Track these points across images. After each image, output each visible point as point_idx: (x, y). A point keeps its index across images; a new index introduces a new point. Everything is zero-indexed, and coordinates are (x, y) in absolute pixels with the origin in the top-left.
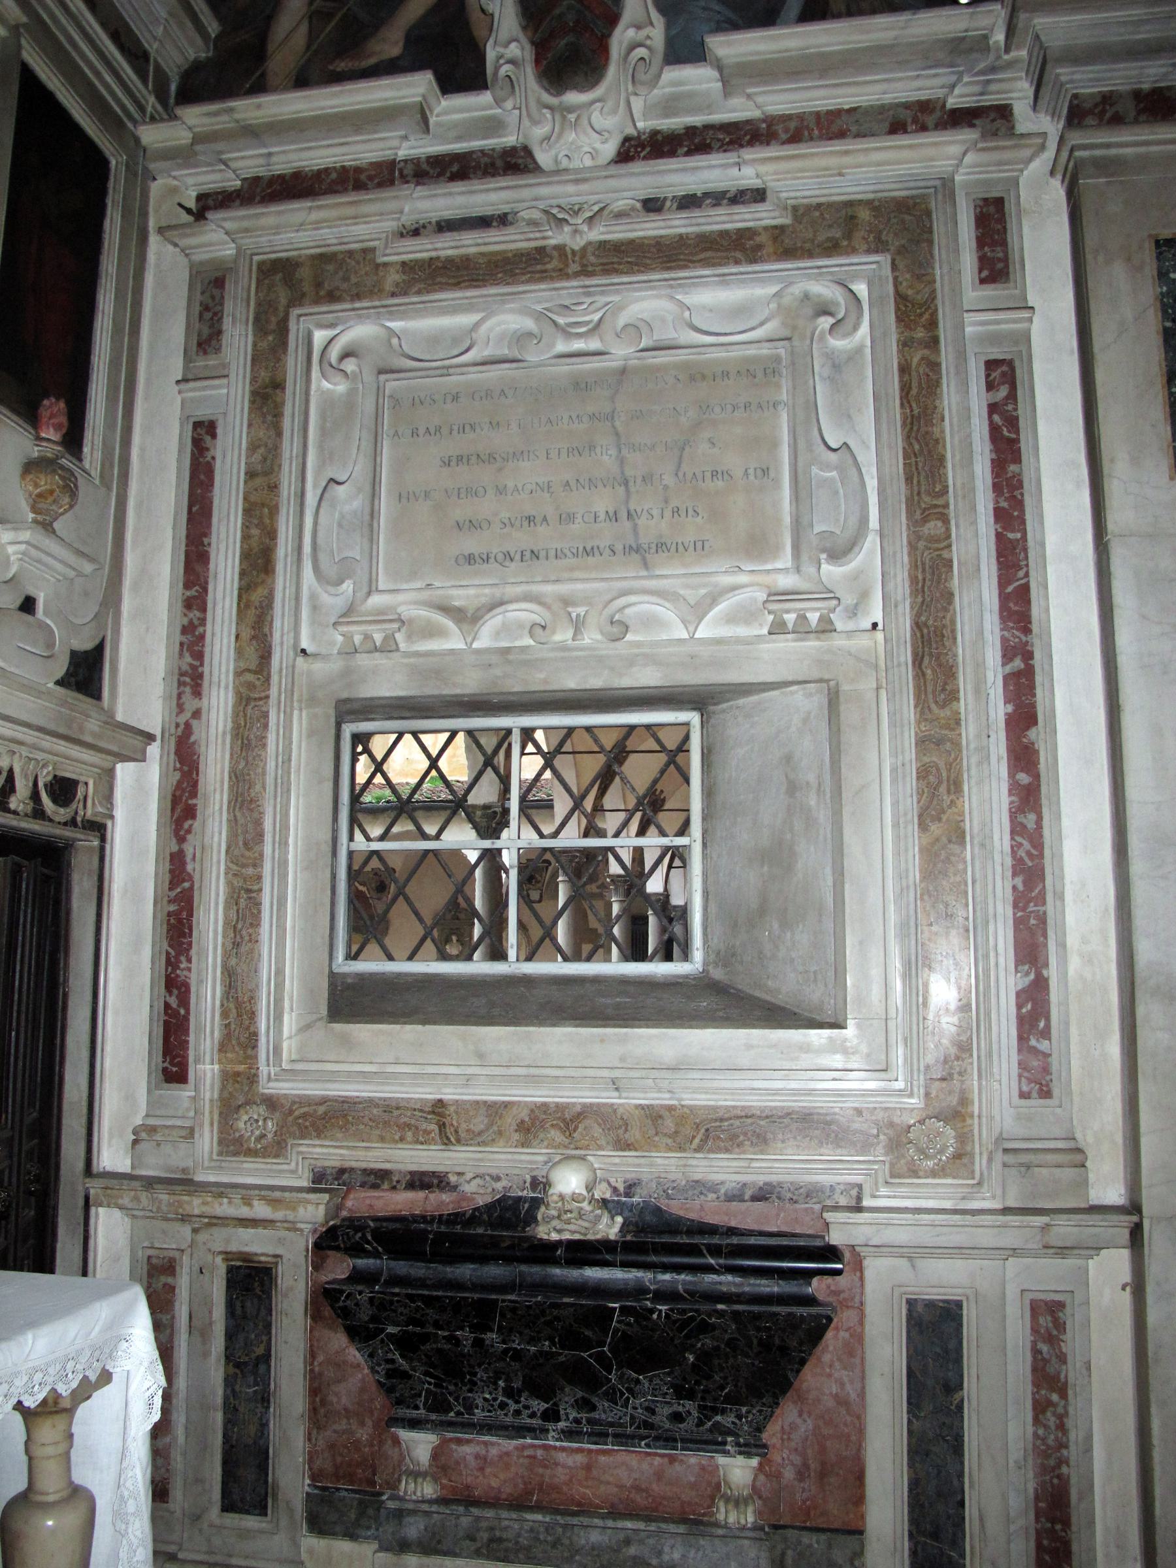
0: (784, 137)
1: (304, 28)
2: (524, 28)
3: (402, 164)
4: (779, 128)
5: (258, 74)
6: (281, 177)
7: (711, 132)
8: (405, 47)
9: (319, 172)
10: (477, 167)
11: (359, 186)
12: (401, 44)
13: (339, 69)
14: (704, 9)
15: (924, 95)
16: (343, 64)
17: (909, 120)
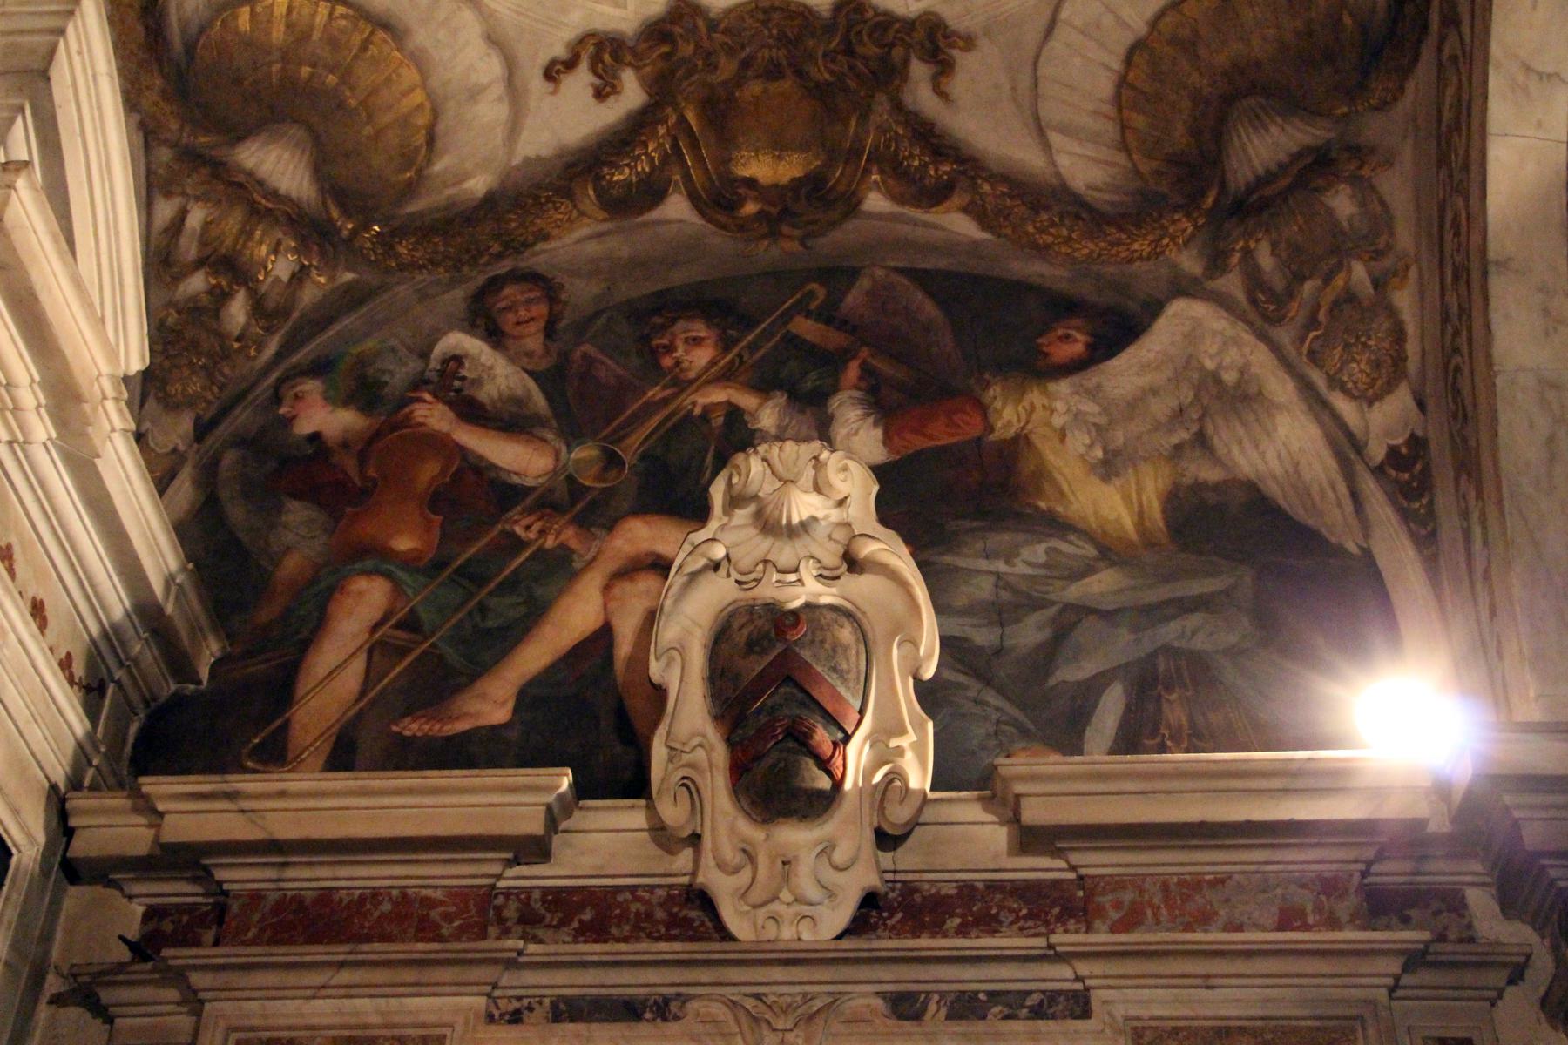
0: (1114, 915)
1: (359, 665)
2: (717, 718)
3: (500, 900)
4: (1105, 900)
5: (278, 722)
6: (298, 900)
7: (998, 897)
8: (515, 710)
9: (362, 900)
10: (623, 918)
11: (427, 930)
12: (511, 705)
13: (407, 733)
14: (976, 701)
15: (1328, 870)
16: (415, 726)
17: (1309, 907)
